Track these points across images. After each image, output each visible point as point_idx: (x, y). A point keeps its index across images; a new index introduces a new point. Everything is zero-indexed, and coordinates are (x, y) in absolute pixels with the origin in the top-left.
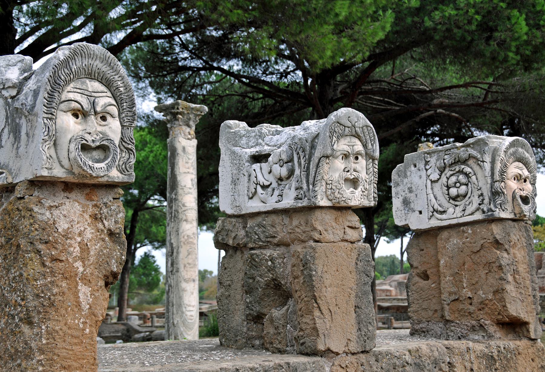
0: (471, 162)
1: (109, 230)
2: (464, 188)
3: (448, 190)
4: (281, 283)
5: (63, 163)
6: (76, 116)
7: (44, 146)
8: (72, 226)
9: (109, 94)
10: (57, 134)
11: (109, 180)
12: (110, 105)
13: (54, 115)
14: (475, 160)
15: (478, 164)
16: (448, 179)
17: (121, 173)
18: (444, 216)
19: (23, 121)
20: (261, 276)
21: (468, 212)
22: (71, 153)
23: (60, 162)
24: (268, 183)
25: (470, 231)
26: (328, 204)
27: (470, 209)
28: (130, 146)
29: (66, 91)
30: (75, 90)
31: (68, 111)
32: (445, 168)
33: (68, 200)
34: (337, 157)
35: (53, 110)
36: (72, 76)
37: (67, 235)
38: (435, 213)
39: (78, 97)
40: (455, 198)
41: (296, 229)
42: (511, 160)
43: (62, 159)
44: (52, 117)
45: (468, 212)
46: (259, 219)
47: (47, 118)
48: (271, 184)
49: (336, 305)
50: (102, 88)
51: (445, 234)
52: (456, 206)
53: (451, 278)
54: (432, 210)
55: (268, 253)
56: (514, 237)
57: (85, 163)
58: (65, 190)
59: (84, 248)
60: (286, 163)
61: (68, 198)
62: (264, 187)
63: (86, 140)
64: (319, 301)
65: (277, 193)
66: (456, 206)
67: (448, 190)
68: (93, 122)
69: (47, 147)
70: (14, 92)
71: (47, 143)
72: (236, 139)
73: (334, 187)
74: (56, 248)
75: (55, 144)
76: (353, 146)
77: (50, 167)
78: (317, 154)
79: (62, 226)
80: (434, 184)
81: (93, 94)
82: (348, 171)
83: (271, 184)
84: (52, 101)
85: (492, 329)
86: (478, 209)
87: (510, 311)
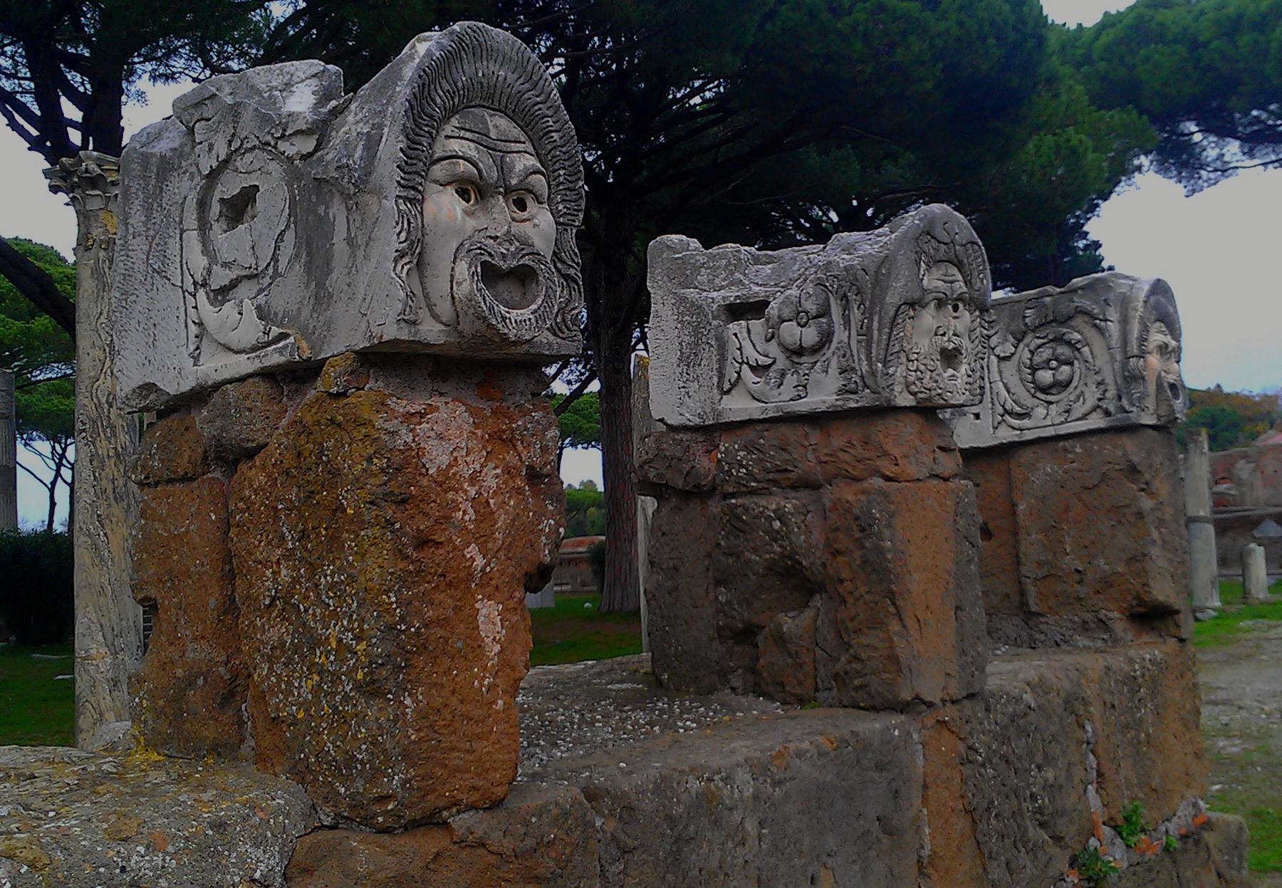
0: (1079, 321)
1: (531, 468)
2: (1066, 368)
3: (1033, 374)
4: (801, 564)
5: (437, 310)
6: (463, 194)
7: (399, 267)
8: (456, 459)
10: (427, 239)
11: (532, 351)
12: (534, 173)
13: (419, 191)
14: (1086, 318)
15: (1095, 326)
16: (1032, 353)
17: (555, 334)
18: (1025, 423)
19: (337, 211)
20: (755, 551)
21: (1075, 415)
22: (459, 284)
23: (431, 307)
24: (770, 361)
25: (1078, 450)
27: (1079, 409)
28: (572, 271)
29: (443, 134)
30: (462, 133)
31: (449, 184)
32: (1024, 334)
33: (443, 399)
35: (419, 180)
36: (456, 100)
37: (446, 481)
38: (1007, 417)
39: (470, 149)
40: (1045, 390)
41: (841, 454)
42: (1153, 318)
43: (435, 299)
44: (414, 196)
45: (1075, 415)
46: (750, 434)
47: (406, 199)
48: (774, 362)
49: (927, 607)
50: (516, 132)
51: (1027, 455)
52: (1050, 403)
53: (1040, 537)
54: (1001, 410)
55: (771, 504)
57: (491, 309)
59: (484, 513)
60: (814, 318)
61: (441, 394)
62: (758, 369)
63: (490, 254)
64: (900, 602)
65: (791, 380)
66: (1050, 403)
67: (1033, 374)
68: (501, 211)
69: (406, 268)
70: (309, 145)
71: (406, 260)
72: (683, 274)
73: (922, 368)
74: (426, 514)
75: (419, 265)
76: (952, 282)
77: (412, 317)
78: (892, 299)
79: (437, 457)
80: (1003, 364)
81: (501, 145)
82: (944, 335)
83: (774, 362)
84: (417, 158)
85: (1120, 625)
86: (1095, 409)
87: (1154, 592)
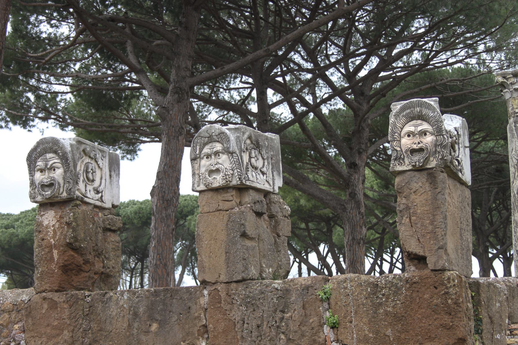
1: (66, 222)
9: (57, 158)
26: (205, 188)
34: (203, 158)
37: (47, 227)
56: (415, 184)
58: (51, 206)
79: (46, 223)
